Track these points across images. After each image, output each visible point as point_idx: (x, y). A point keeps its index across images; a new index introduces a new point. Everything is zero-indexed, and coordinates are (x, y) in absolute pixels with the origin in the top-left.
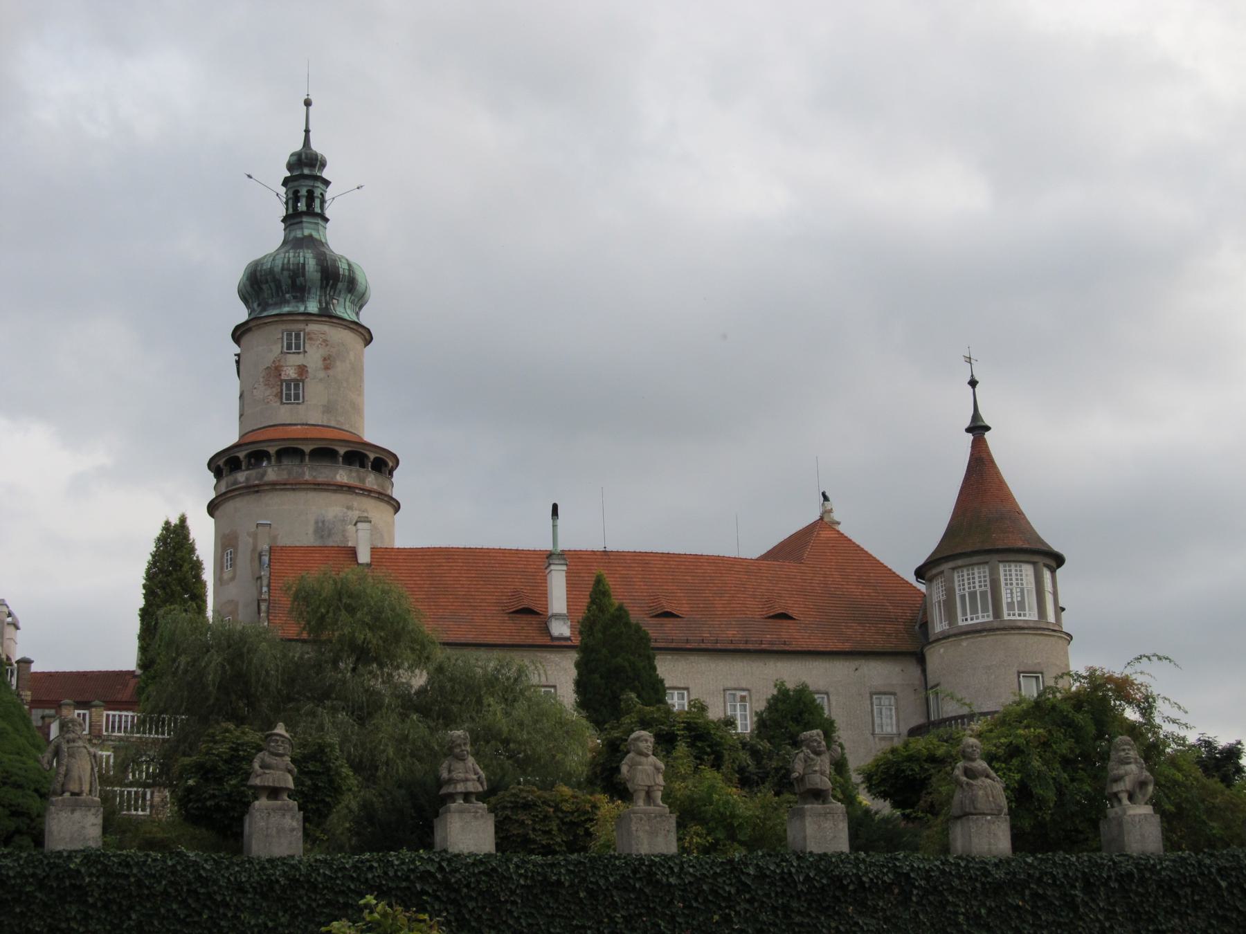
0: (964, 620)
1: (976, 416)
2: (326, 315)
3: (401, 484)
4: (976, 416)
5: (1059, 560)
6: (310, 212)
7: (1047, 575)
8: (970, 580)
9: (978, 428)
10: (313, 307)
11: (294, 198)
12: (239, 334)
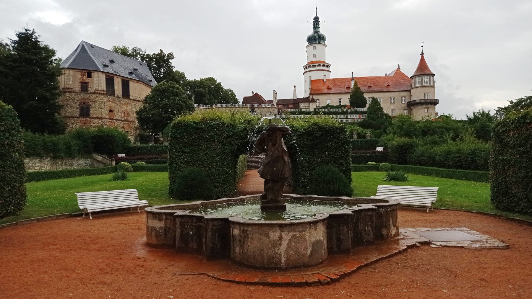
0: (417, 85)
1: (422, 52)
2: (319, 43)
3: (331, 69)
4: (422, 52)
5: (434, 75)
6: (317, 27)
7: (432, 77)
8: (418, 79)
9: (422, 54)
10: (317, 42)
11: (314, 24)
12: (306, 47)
